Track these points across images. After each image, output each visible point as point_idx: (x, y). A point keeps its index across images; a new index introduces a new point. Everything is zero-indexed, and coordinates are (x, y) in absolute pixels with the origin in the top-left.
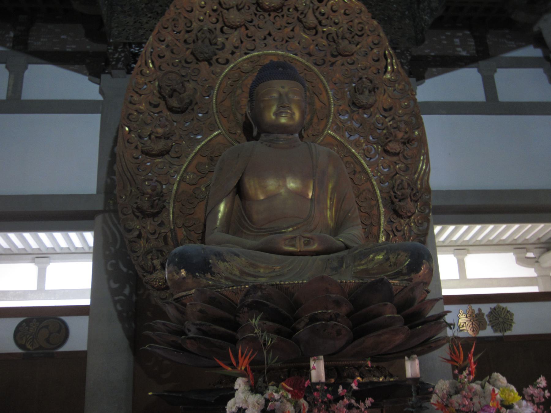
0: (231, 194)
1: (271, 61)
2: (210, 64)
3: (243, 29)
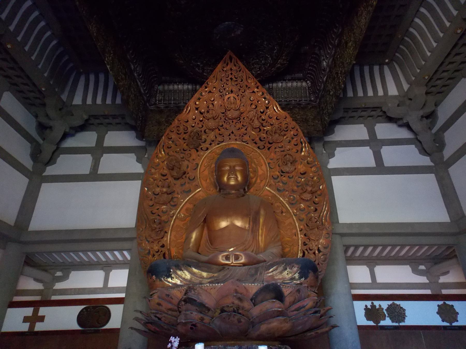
0: (200, 227)
2: (197, 151)
3: (217, 130)
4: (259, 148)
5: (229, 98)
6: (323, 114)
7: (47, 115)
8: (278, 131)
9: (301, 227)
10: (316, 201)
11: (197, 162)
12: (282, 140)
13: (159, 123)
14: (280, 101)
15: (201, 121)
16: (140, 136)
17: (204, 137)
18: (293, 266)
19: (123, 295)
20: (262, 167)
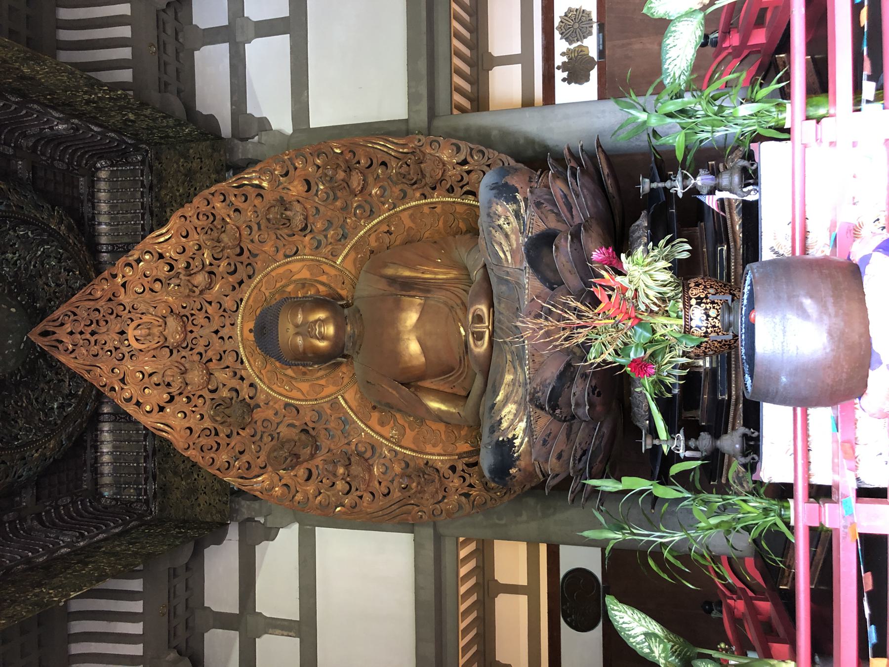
0: (419, 394)
1: (251, 331)
2: (258, 406)
3: (210, 365)
4: (250, 277)
5: (137, 340)
6: (175, 138)
8: (215, 234)
9: (418, 195)
10: (367, 163)
11: (282, 407)
12: (234, 227)
13: (193, 491)
14: (143, 229)
15: (187, 397)
16: (217, 532)
17: (225, 393)
18: (495, 214)
19: (543, 548)
20: (293, 270)
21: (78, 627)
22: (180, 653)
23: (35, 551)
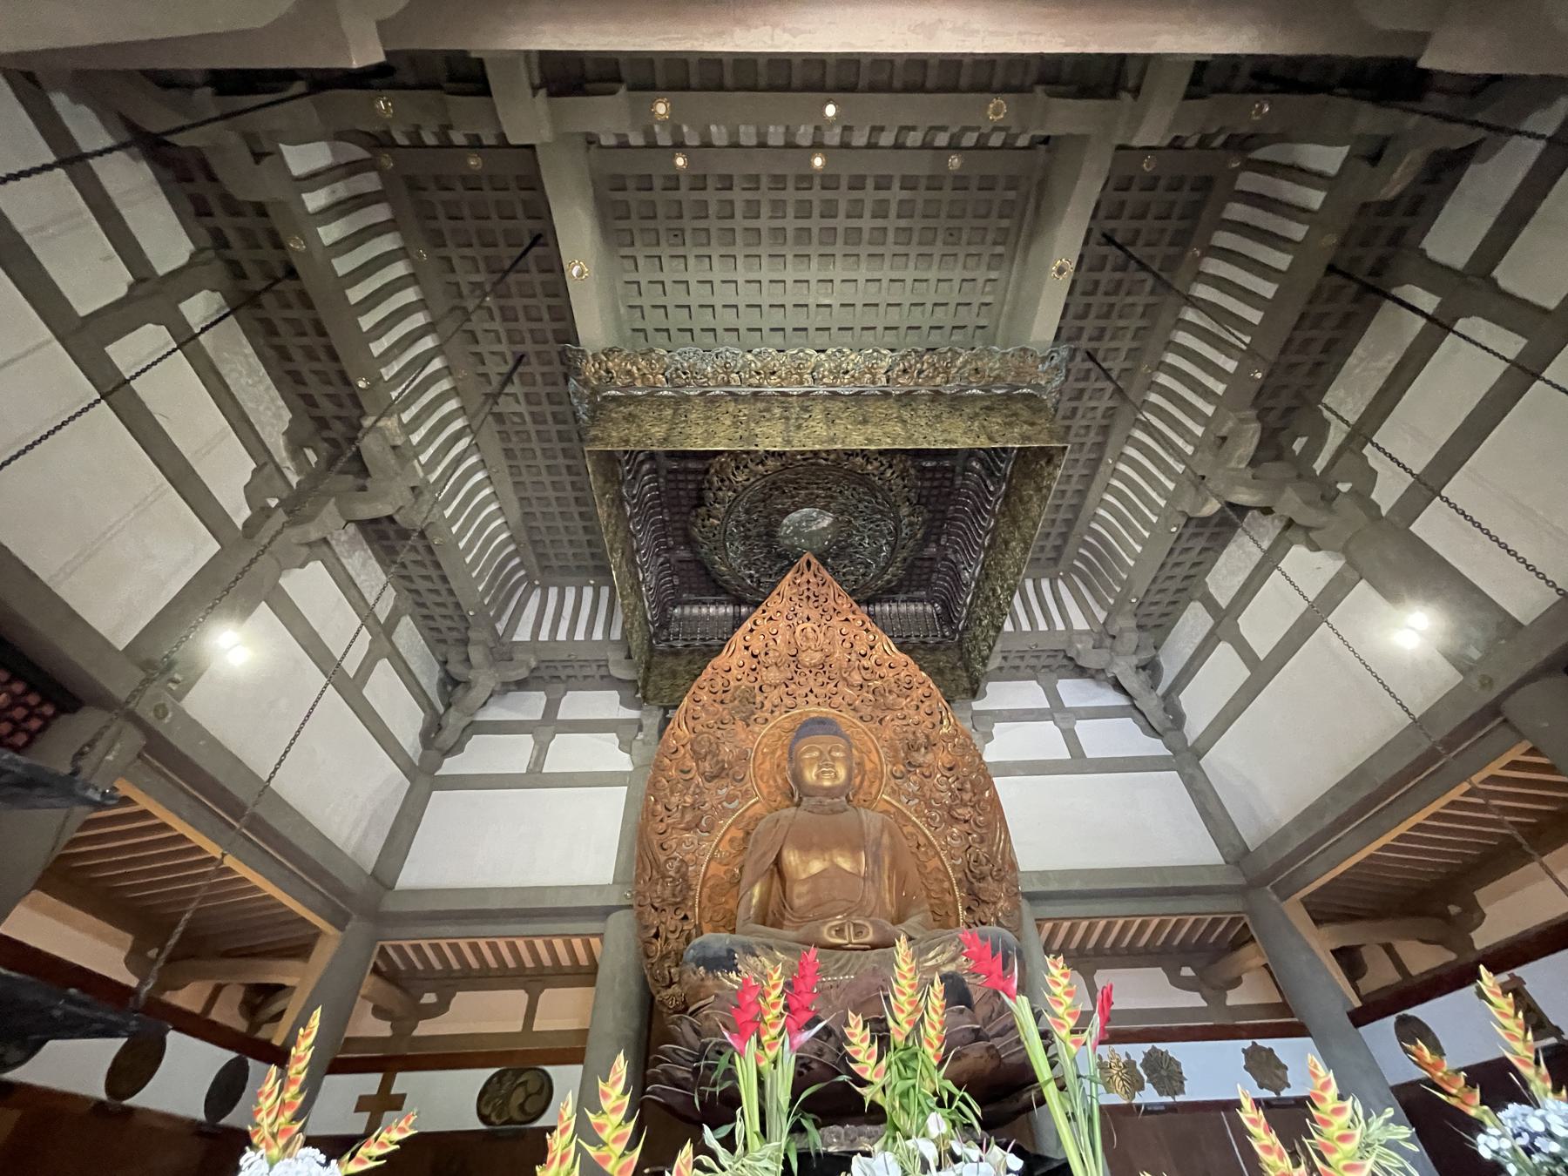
2: (748, 725)
7: (468, 659)
9: (960, 875)
17: (759, 699)
21: (570, 593)
22: (533, 671)
23: (645, 555)
